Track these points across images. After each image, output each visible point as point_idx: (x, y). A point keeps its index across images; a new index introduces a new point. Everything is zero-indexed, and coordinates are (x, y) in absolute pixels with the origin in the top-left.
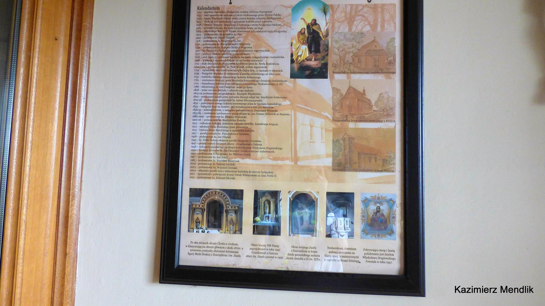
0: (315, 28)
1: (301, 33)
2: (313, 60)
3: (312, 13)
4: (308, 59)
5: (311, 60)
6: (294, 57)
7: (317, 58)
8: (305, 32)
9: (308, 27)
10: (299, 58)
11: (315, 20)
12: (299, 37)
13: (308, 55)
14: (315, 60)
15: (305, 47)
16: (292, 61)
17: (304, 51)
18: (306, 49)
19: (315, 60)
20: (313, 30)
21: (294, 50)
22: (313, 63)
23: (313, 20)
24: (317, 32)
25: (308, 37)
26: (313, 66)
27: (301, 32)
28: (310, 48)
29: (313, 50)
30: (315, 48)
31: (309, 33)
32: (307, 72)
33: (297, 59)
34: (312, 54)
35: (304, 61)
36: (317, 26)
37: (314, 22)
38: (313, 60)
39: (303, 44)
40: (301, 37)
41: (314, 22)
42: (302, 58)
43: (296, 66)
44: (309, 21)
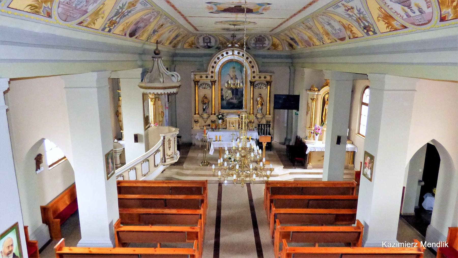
4: (231, 99)
6: (224, 98)
16: (222, 99)
17: (228, 94)
21: (224, 93)
22: (235, 101)
29: (234, 93)
32: (231, 106)
35: (229, 99)
43: (225, 102)
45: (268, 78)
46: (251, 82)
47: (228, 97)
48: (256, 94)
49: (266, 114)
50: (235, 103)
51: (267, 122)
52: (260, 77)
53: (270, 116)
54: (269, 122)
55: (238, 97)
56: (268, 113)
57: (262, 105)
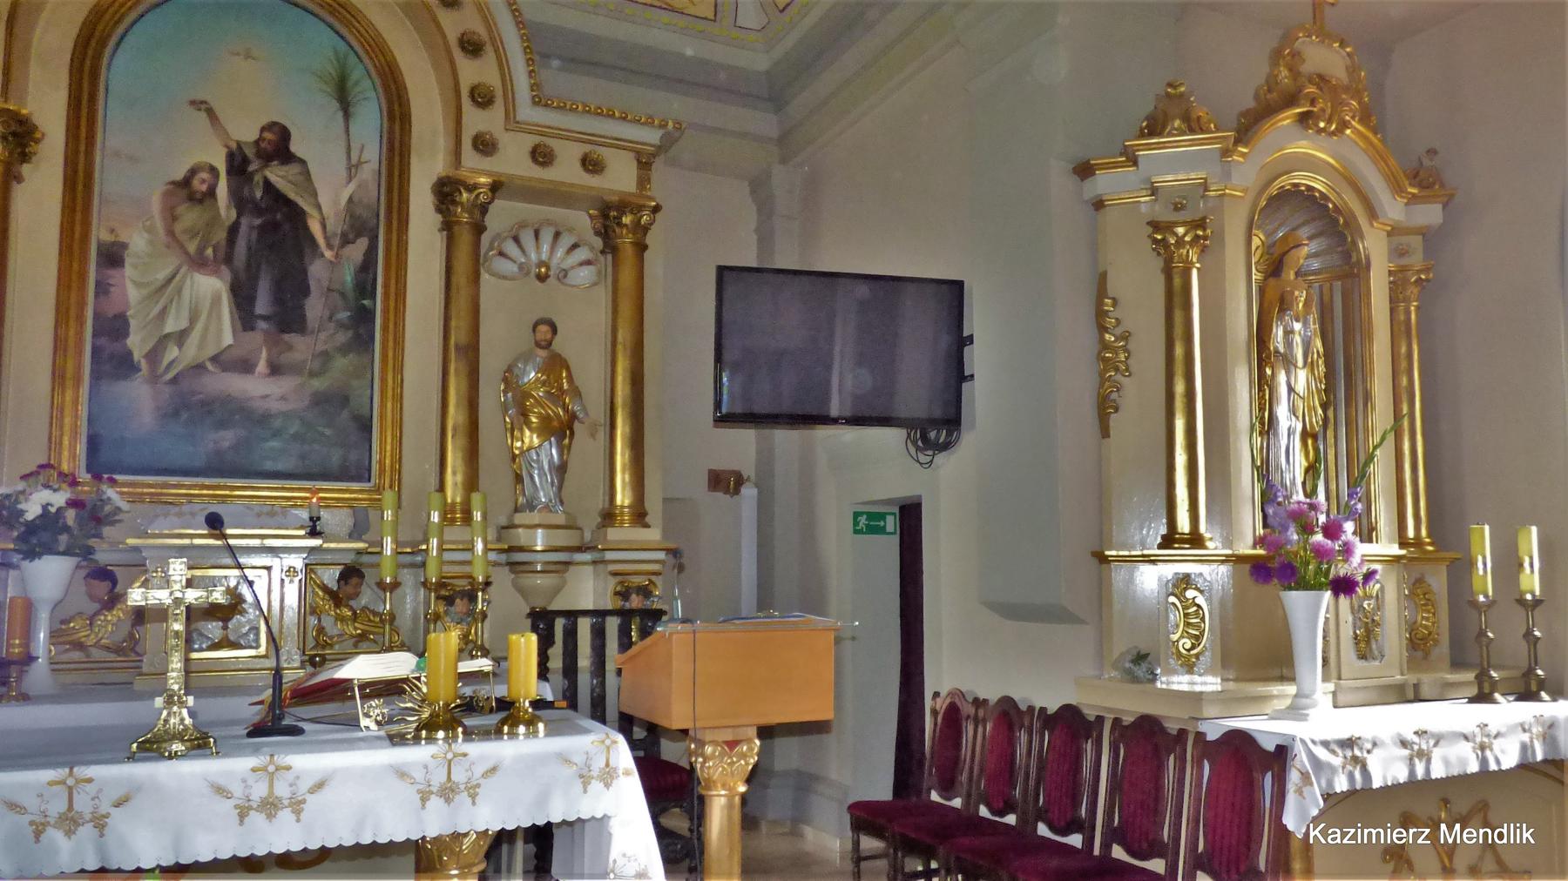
0: (278, 175)
1: (188, 191)
2: (262, 367)
3: (264, 83)
5: (245, 366)
7: (287, 358)
8: (211, 193)
9: (238, 164)
10: (172, 352)
11: (284, 134)
12: (171, 217)
13: (228, 339)
14: (275, 370)
15: (211, 286)
18: (216, 301)
19: (275, 370)
20: (268, 186)
21: (133, 294)
23: (271, 126)
24: (289, 203)
25: (233, 230)
26: (259, 405)
27: (186, 182)
28: (242, 296)
29: (262, 305)
30: (278, 299)
31: (240, 202)
33: (154, 355)
34: (256, 338)
35: (199, 368)
36: (293, 169)
37: (278, 145)
38: (262, 367)
39: (199, 263)
40: (190, 217)
41: (278, 145)
42: (191, 352)
43: (139, 399)
44: (246, 132)
45: (620, 177)
46: (446, 192)
47: (181, 337)
48: (501, 336)
49: (609, 516)
50: (275, 406)
51: (624, 595)
52: (541, 156)
53: (653, 535)
54: (645, 592)
55: (301, 347)
56: (623, 498)
57: (561, 430)
